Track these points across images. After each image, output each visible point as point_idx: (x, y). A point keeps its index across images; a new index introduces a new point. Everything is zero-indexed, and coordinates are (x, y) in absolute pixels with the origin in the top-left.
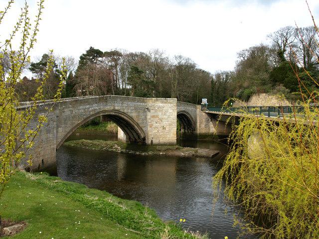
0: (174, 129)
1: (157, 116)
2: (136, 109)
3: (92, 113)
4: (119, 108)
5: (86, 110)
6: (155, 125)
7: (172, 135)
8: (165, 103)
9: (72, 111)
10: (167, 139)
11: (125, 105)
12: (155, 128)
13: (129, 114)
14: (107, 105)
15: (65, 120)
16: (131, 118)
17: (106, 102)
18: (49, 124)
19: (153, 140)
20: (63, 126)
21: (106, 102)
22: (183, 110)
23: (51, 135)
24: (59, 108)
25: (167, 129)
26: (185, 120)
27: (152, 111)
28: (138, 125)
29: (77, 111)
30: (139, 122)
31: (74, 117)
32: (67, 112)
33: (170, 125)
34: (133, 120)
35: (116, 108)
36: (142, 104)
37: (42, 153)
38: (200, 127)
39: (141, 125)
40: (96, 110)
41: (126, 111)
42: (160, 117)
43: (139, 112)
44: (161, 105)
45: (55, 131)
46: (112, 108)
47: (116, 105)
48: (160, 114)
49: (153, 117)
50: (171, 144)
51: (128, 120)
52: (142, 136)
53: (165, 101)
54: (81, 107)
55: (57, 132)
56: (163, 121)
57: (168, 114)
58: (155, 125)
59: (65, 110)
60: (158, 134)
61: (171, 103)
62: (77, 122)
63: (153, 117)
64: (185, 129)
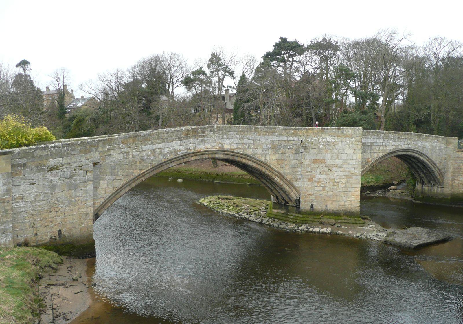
0: (355, 186)
1: (323, 161)
2: (274, 148)
3: (169, 157)
4: (235, 147)
5: (158, 151)
6: (318, 176)
7: (353, 198)
8: (339, 136)
9: (128, 154)
10: (342, 203)
11: (248, 142)
12: (318, 183)
13: (257, 157)
14: (203, 141)
15: (113, 168)
16: (264, 164)
17: (203, 136)
18: (72, 176)
19: (315, 205)
20: (109, 177)
21: (203, 136)
22: (407, 147)
23: (79, 193)
24: (100, 149)
25: (341, 186)
26: (419, 167)
27: (312, 151)
28: (281, 176)
29: (138, 153)
30: (285, 171)
31: (132, 163)
32: (116, 156)
33: (347, 178)
34: (269, 166)
35: (227, 147)
36: (291, 138)
37: (59, 220)
38: (453, 180)
39: (288, 177)
40: (179, 150)
41: (249, 152)
42: (328, 162)
43: (284, 153)
44: (330, 139)
45: (90, 187)
46: (216, 148)
47: (226, 141)
48: (328, 157)
49: (315, 161)
50: (349, 214)
51: (258, 167)
52: (294, 196)
53: (340, 132)
54: (145, 146)
55: (96, 188)
56: (334, 169)
57: (343, 157)
58: (318, 176)
59: (112, 152)
60: (323, 194)
61: (350, 137)
62: (137, 173)
63: (315, 161)
64: (423, 183)
